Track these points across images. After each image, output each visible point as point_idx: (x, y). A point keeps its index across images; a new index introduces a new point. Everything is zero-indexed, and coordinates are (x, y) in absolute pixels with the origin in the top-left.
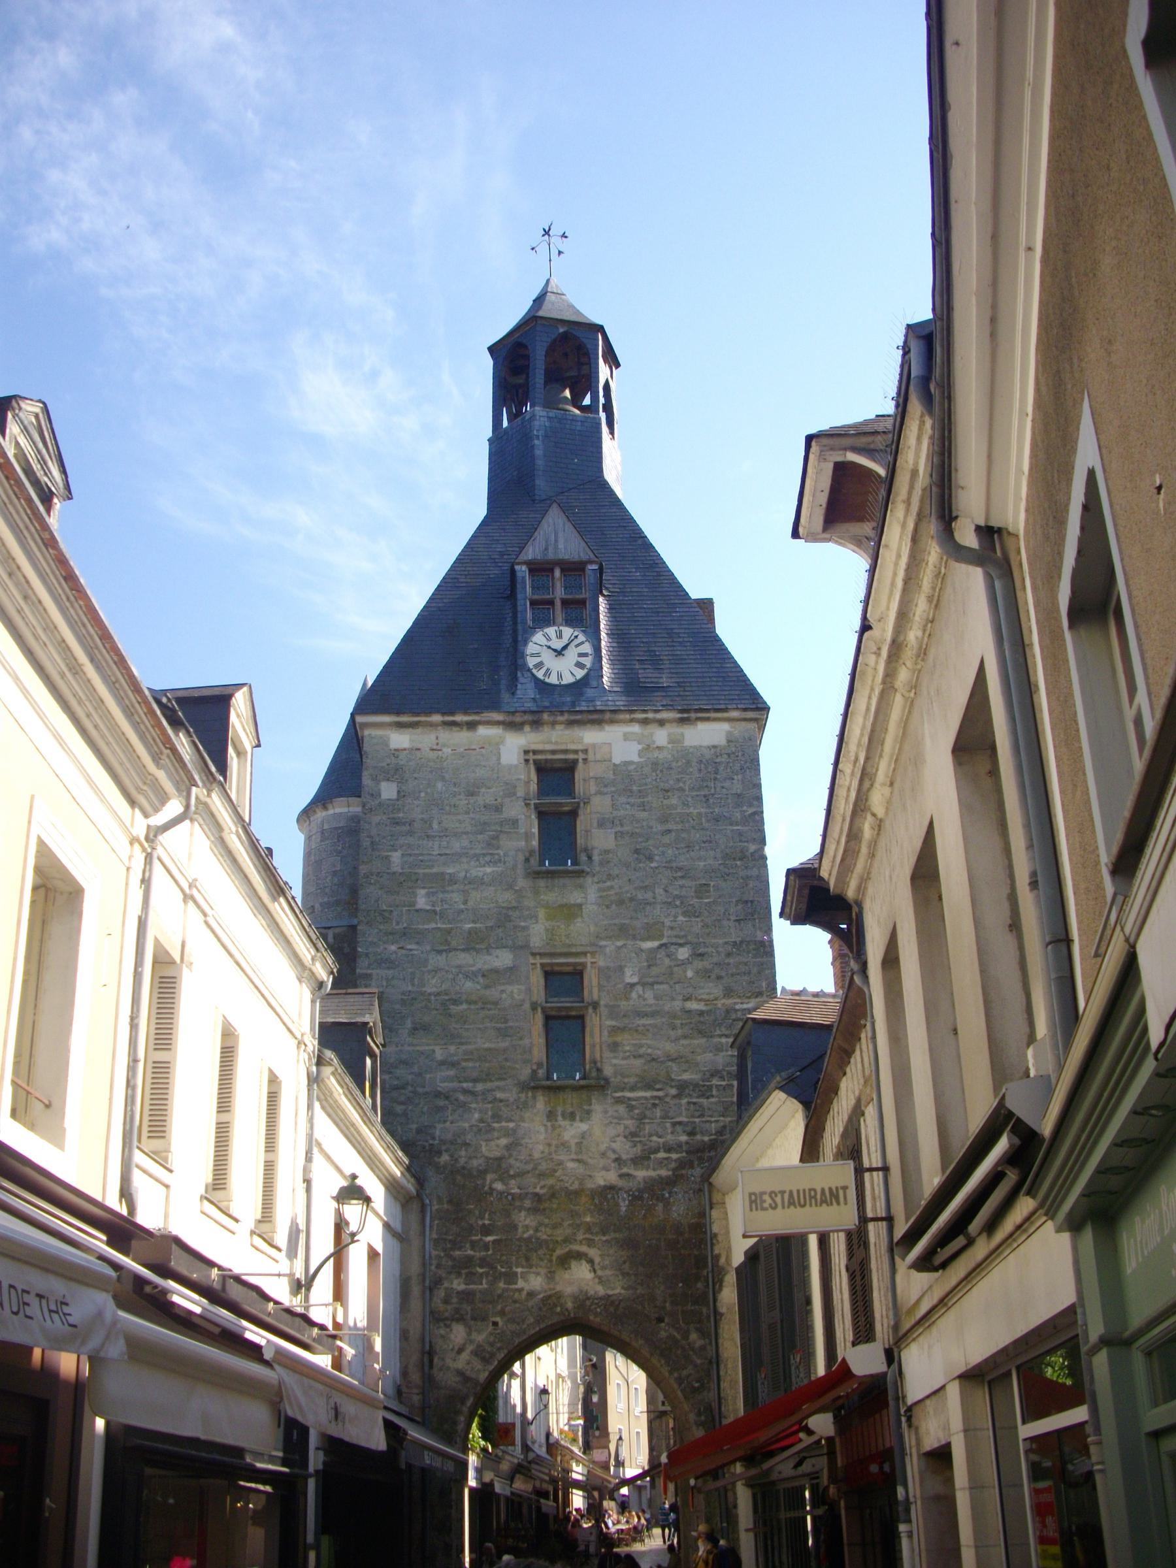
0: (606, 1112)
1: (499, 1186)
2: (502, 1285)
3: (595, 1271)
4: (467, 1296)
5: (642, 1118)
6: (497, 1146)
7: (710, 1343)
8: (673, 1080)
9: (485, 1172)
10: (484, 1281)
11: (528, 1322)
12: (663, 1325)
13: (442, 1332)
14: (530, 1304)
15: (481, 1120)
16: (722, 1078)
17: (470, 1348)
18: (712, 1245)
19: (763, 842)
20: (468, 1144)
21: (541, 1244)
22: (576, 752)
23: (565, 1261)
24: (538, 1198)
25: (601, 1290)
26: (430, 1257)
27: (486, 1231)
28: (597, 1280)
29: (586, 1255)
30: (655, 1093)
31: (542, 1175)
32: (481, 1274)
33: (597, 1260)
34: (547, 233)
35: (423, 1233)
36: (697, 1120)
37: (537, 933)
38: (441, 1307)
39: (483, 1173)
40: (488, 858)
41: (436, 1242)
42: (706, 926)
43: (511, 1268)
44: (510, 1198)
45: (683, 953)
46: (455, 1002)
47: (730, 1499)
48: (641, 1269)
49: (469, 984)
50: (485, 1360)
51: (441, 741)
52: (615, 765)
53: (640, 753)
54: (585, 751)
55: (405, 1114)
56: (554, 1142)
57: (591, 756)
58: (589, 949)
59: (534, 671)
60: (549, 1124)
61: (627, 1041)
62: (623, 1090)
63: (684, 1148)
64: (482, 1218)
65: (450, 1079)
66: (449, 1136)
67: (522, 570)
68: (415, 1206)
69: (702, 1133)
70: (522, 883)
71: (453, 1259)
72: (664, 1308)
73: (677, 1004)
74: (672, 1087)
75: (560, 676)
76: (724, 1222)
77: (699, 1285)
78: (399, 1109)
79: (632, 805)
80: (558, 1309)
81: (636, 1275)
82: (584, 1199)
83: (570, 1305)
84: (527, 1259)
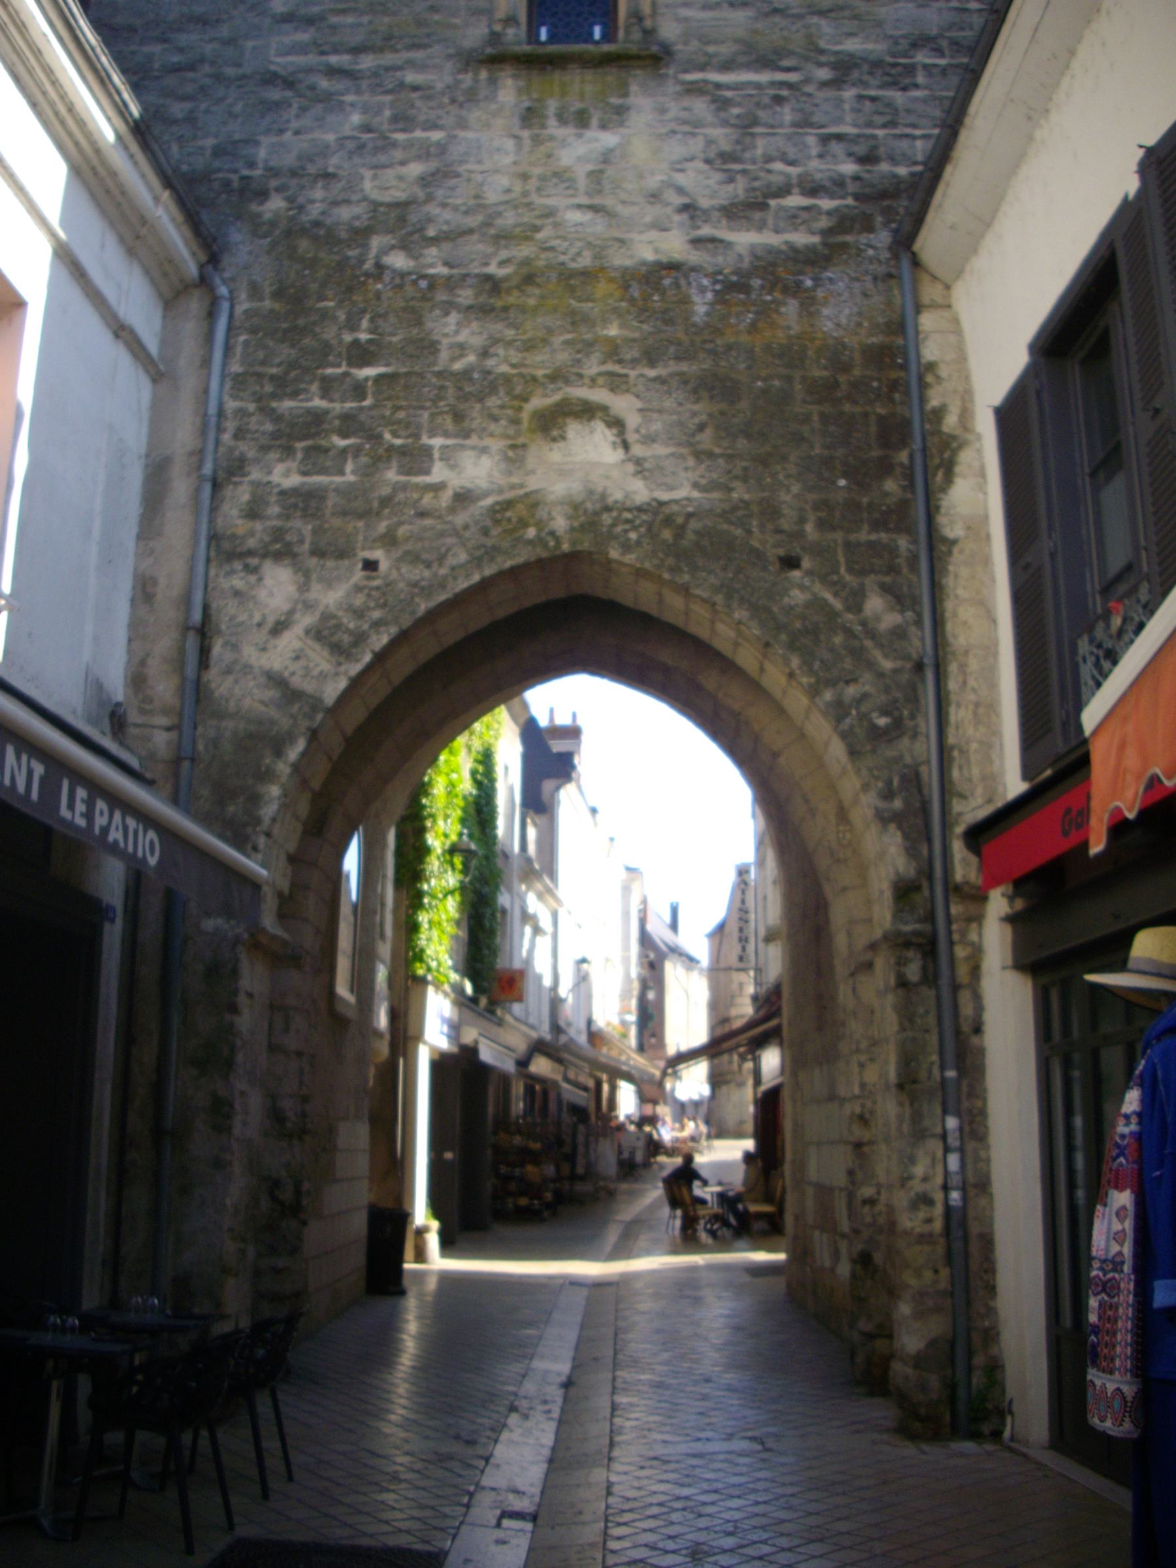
0: (663, 111)
1: (399, 261)
2: (392, 475)
3: (626, 446)
4: (304, 502)
5: (747, 124)
6: (401, 178)
7: (919, 622)
8: (822, 52)
10: (349, 467)
11: (451, 561)
12: (796, 574)
13: (237, 582)
14: (460, 519)
15: (367, 128)
16: (939, 52)
17: (306, 620)
18: (923, 386)
20: (333, 176)
21: (492, 384)
23: (550, 423)
24: (493, 285)
25: (640, 491)
26: (221, 414)
27: (362, 355)
28: (631, 468)
29: (605, 409)
30: (780, 76)
31: (503, 238)
32: (344, 451)
33: (633, 420)
35: (206, 362)
36: (880, 133)
38: (241, 526)
39: (361, 235)
41: (239, 382)
43: (417, 436)
44: (423, 284)
47: (967, 1010)
48: (742, 443)
50: (340, 651)
55: (191, 119)
56: (537, 171)
60: (526, 134)
62: (702, 68)
63: (851, 187)
64: (353, 327)
65: (301, 49)
66: (289, 160)
68: (195, 304)
69: (893, 160)
71: (277, 418)
72: (800, 535)
74: (820, 65)
76: (952, 339)
77: (890, 485)
78: (178, 109)
80: (531, 532)
81: (730, 458)
82: (602, 288)
83: (560, 524)
84: (458, 417)
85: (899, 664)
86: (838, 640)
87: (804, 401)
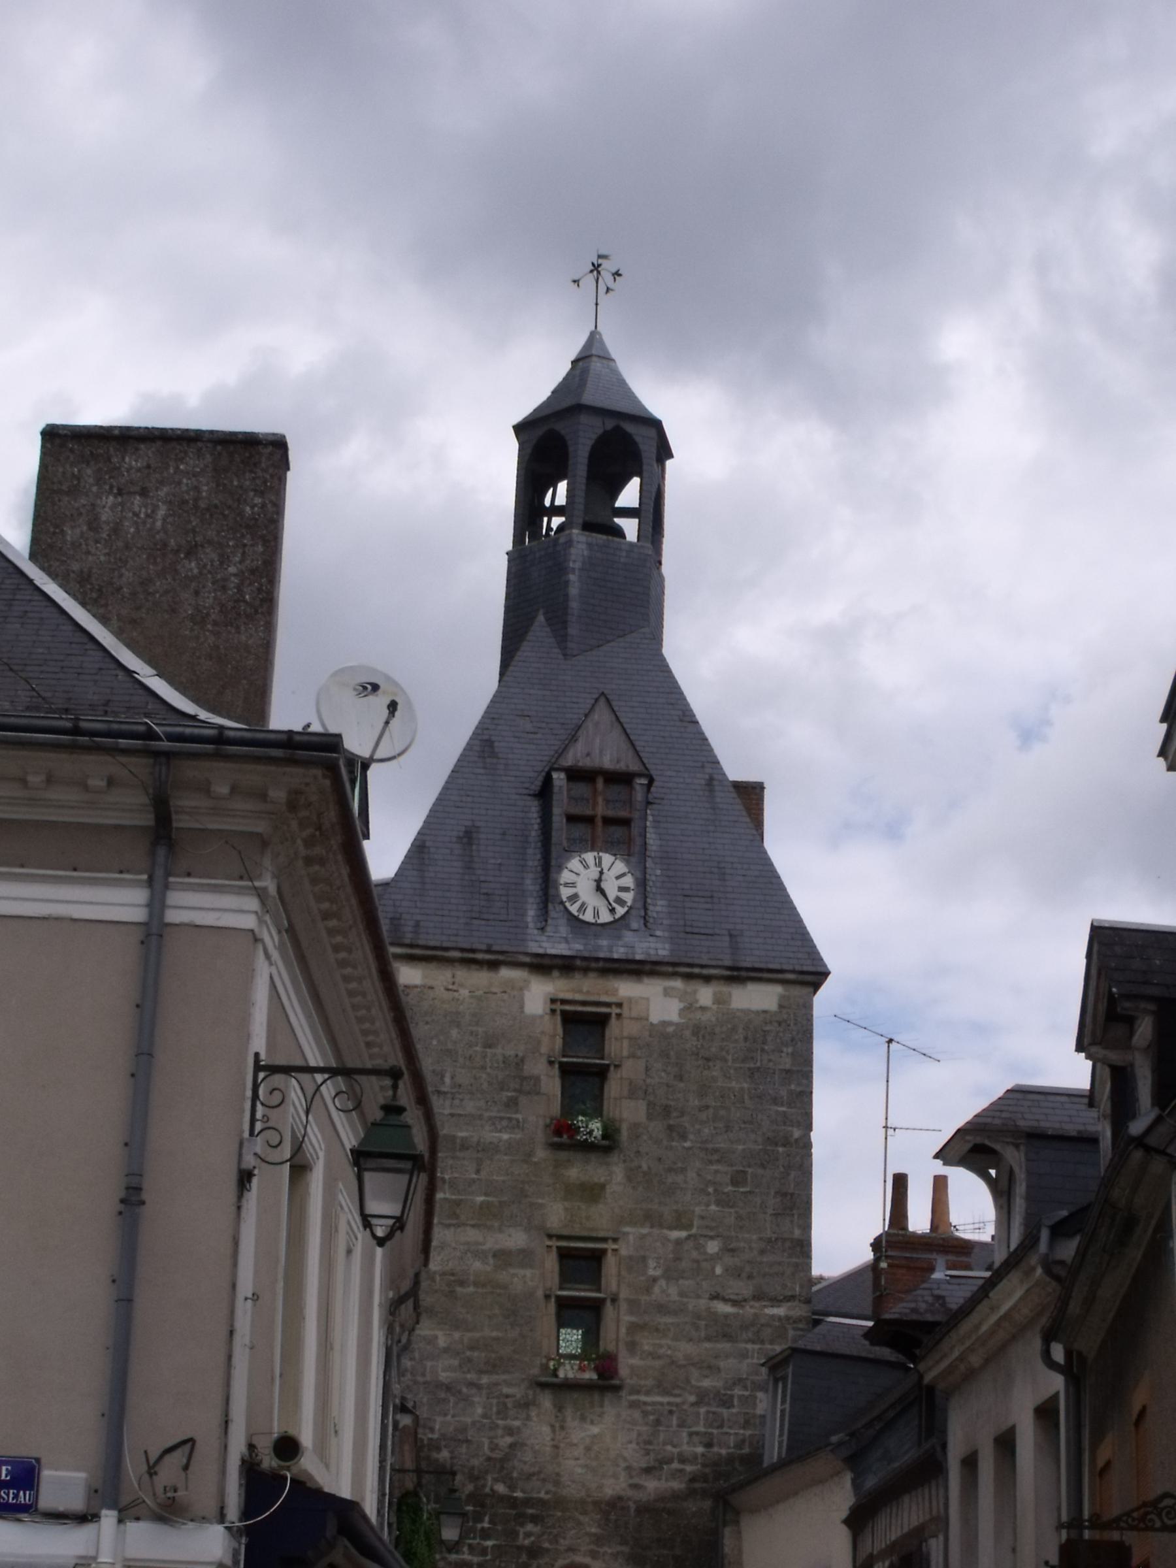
9: (487, 1472)
15: (485, 1416)
19: (809, 1127)
22: (608, 1005)
27: (485, 1535)
30: (672, 1399)
34: (596, 268)
36: (715, 1431)
37: (556, 1214)
40: (505, 1123)
42: (739, 1217)
45: (713, 1247)
46: (462, 1283)
49: (477, 1265)
51: (457, 980)
52: (652, 1024)
53: (682, 1012)
54: (620, 1005)
57: (625, 1012)
58: (610, 1234)
59: (567, 904)
61: (647, 1343)
62: (638, 1392)
67: (559, 778)
69: (720, 1446)
70: (541, 1154)
73: (703, 1303)
74: (691, 1394)
75: (596, 913)
79: (668, 1074)
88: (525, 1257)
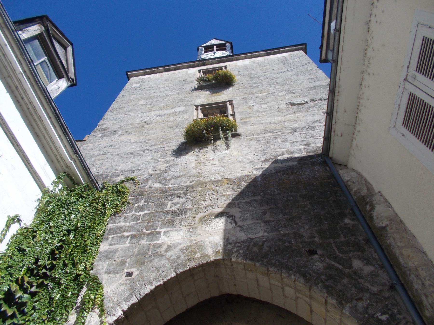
3: (236, 223)
9: (148, 180)
12: (316, 256)
27: (141, 209)
28: (238, 229)
32: (128, 237)
36: (309, 139)
80: (198, 255)
85: (381, 288)
86: (345, 281)
87: (303, 201)
88: (184, 112)
